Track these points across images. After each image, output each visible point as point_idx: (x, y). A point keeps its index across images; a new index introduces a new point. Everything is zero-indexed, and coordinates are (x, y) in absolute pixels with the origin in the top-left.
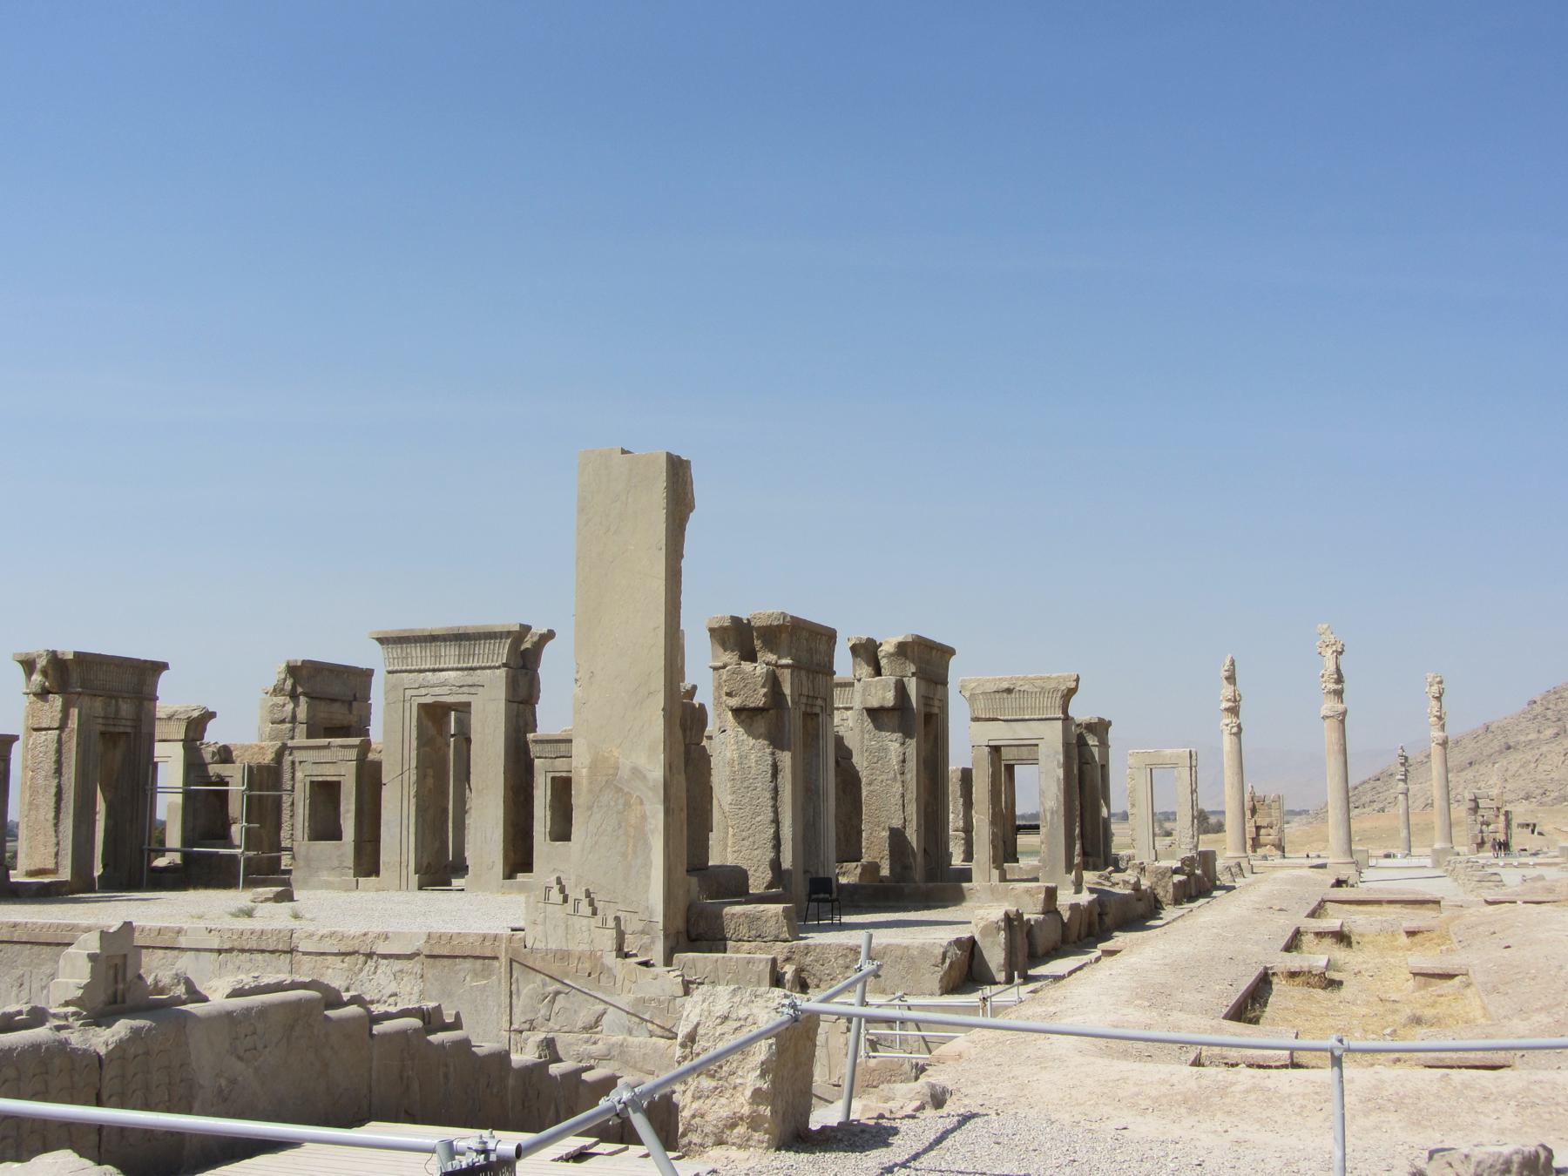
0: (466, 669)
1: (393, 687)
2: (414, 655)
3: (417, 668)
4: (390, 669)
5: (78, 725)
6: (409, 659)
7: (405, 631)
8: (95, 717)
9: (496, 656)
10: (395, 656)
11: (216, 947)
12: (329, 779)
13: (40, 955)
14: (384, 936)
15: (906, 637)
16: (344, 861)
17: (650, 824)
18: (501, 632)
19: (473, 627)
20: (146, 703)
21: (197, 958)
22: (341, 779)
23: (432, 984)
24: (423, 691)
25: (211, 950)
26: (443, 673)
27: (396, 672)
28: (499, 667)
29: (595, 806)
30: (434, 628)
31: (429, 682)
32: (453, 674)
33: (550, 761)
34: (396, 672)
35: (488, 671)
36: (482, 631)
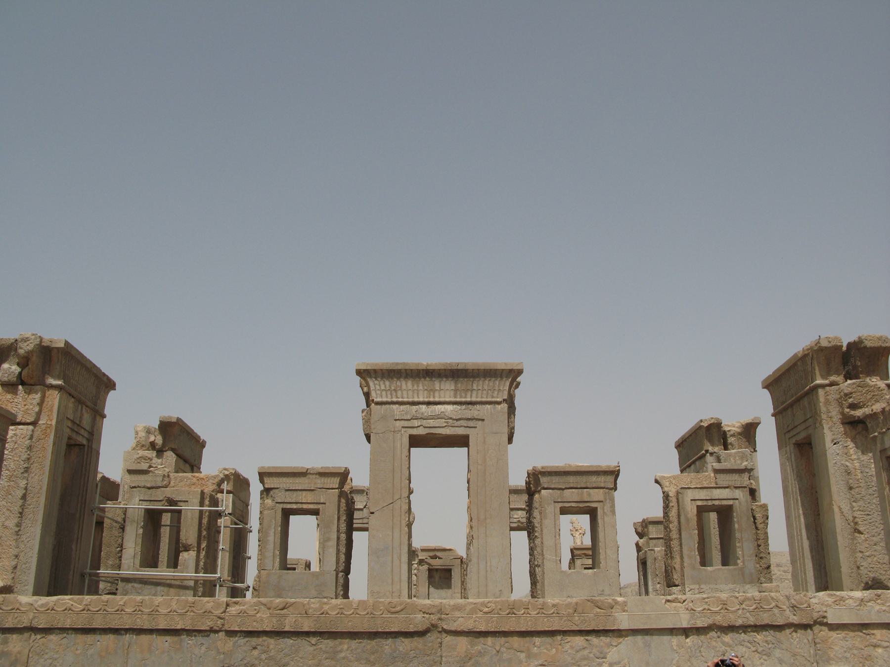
2: (404, 387)
3: (411, 400)
4: (379, 399)
5: (57, 422)
6: (399, 393)
7: (397, 364)
8: (67, 417)
9: (496, 393)
10: (383, 387)
11: (685, 625)
12: (305, 506)
13: (336, 653)
16: (323, 591)
18: (503, 370)
19: (473, 364)
20: (98, 418)
24: (416, 423)
25: (672, 631)
26: (439, 406)
28: (499, 403)
30: (429, 363)
31: (422, 414)
32: (449, 408)
33: (559, 492)
35: (489, 406)
36: (483, 368)
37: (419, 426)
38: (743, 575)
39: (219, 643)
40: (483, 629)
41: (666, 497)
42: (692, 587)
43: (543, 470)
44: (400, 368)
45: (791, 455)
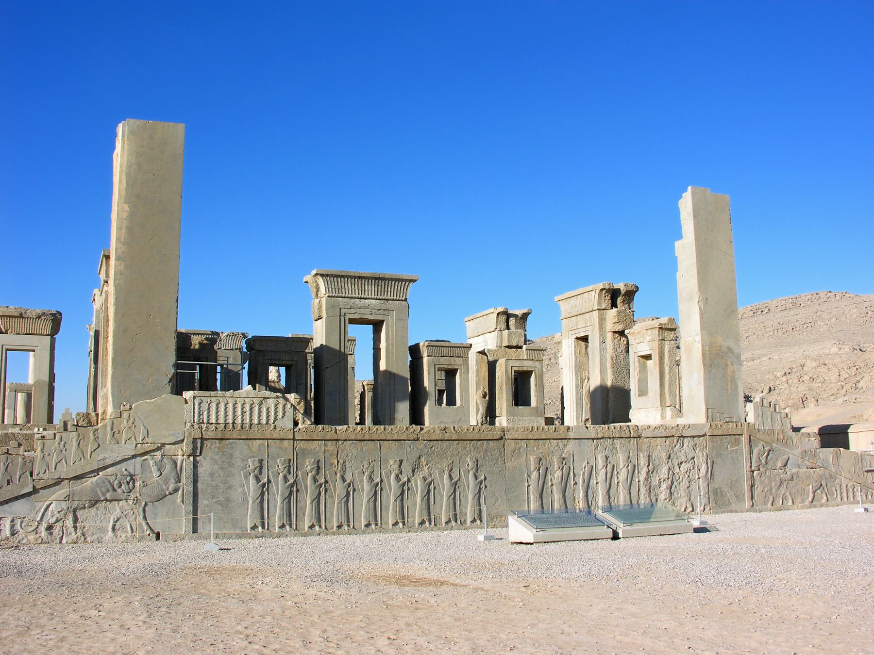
0: (383, 300)
1: (332, 306)
7: (342, 271)
14: (688, 426)
15: (528, 310)
17: (737, 375)
21: (580, 445)
22: (294, 363)
23: (712, 451)
24: (353, 311)
26: (367, 300)
27: (334, 297)
28: (403, 301)
29: (713, 367)
31: (357, 305)
34: (334, 297)
35: (396, 302)
37: (354, 313)
38: (537, 413)
39: (418, 445)
40: (521, 438)
41: (489, 362)
42: (509, 418)
43: (429, 345)
44: (344, 274)
45: (572, 344)
